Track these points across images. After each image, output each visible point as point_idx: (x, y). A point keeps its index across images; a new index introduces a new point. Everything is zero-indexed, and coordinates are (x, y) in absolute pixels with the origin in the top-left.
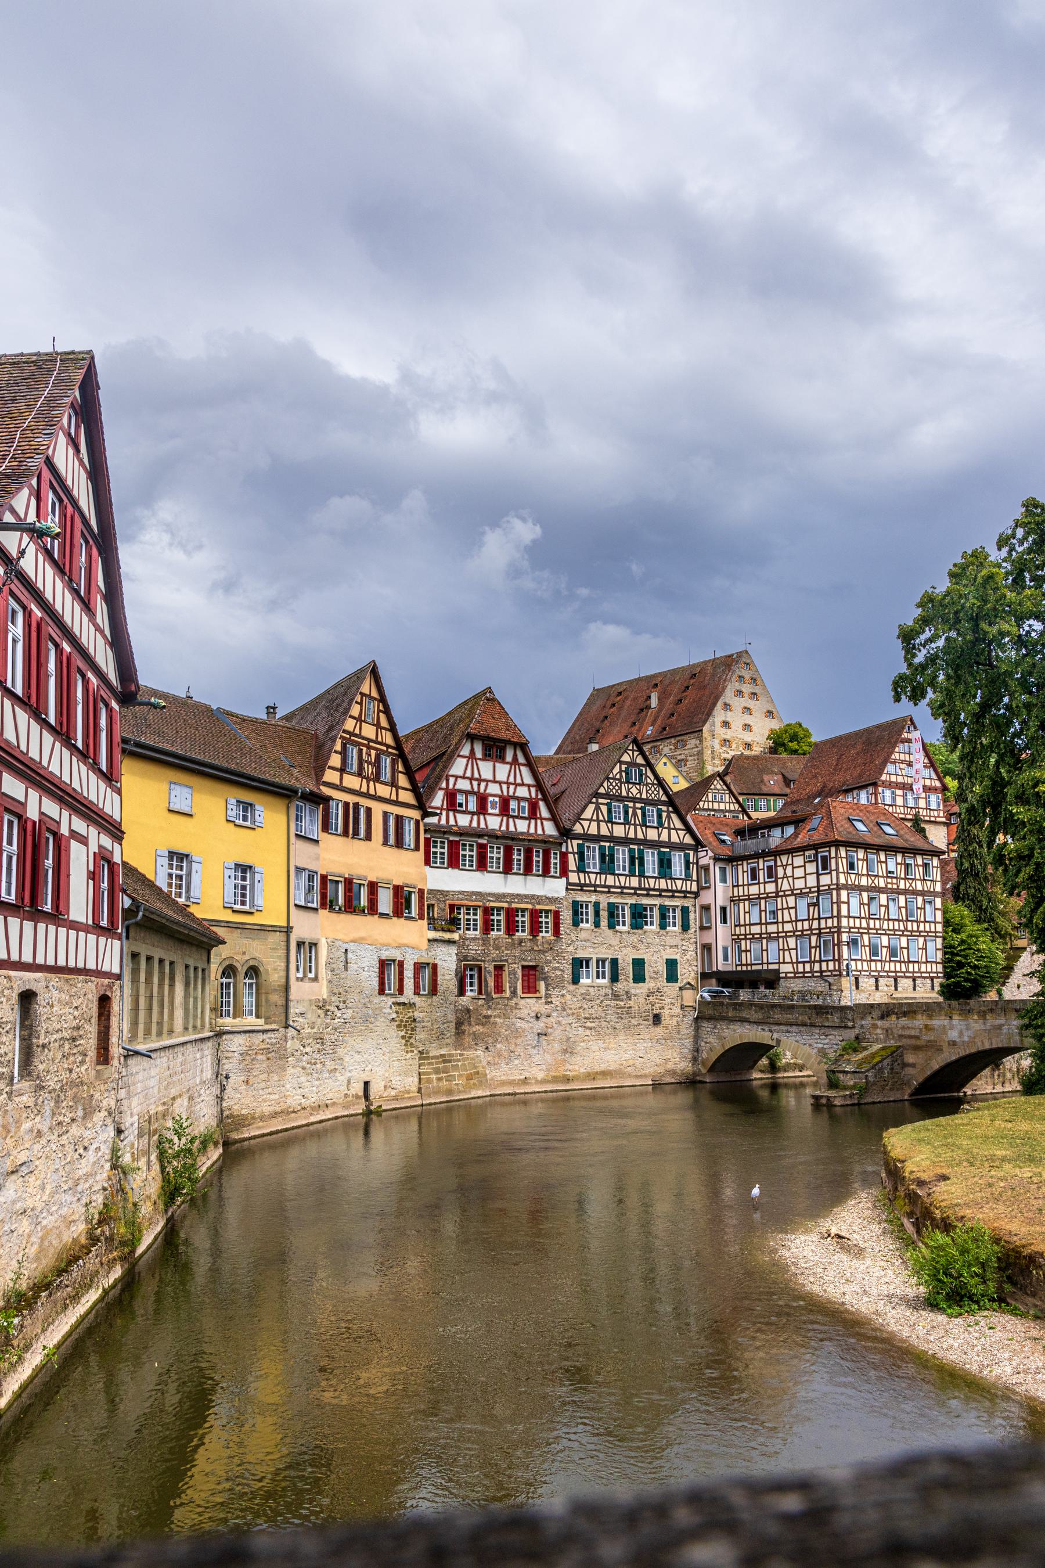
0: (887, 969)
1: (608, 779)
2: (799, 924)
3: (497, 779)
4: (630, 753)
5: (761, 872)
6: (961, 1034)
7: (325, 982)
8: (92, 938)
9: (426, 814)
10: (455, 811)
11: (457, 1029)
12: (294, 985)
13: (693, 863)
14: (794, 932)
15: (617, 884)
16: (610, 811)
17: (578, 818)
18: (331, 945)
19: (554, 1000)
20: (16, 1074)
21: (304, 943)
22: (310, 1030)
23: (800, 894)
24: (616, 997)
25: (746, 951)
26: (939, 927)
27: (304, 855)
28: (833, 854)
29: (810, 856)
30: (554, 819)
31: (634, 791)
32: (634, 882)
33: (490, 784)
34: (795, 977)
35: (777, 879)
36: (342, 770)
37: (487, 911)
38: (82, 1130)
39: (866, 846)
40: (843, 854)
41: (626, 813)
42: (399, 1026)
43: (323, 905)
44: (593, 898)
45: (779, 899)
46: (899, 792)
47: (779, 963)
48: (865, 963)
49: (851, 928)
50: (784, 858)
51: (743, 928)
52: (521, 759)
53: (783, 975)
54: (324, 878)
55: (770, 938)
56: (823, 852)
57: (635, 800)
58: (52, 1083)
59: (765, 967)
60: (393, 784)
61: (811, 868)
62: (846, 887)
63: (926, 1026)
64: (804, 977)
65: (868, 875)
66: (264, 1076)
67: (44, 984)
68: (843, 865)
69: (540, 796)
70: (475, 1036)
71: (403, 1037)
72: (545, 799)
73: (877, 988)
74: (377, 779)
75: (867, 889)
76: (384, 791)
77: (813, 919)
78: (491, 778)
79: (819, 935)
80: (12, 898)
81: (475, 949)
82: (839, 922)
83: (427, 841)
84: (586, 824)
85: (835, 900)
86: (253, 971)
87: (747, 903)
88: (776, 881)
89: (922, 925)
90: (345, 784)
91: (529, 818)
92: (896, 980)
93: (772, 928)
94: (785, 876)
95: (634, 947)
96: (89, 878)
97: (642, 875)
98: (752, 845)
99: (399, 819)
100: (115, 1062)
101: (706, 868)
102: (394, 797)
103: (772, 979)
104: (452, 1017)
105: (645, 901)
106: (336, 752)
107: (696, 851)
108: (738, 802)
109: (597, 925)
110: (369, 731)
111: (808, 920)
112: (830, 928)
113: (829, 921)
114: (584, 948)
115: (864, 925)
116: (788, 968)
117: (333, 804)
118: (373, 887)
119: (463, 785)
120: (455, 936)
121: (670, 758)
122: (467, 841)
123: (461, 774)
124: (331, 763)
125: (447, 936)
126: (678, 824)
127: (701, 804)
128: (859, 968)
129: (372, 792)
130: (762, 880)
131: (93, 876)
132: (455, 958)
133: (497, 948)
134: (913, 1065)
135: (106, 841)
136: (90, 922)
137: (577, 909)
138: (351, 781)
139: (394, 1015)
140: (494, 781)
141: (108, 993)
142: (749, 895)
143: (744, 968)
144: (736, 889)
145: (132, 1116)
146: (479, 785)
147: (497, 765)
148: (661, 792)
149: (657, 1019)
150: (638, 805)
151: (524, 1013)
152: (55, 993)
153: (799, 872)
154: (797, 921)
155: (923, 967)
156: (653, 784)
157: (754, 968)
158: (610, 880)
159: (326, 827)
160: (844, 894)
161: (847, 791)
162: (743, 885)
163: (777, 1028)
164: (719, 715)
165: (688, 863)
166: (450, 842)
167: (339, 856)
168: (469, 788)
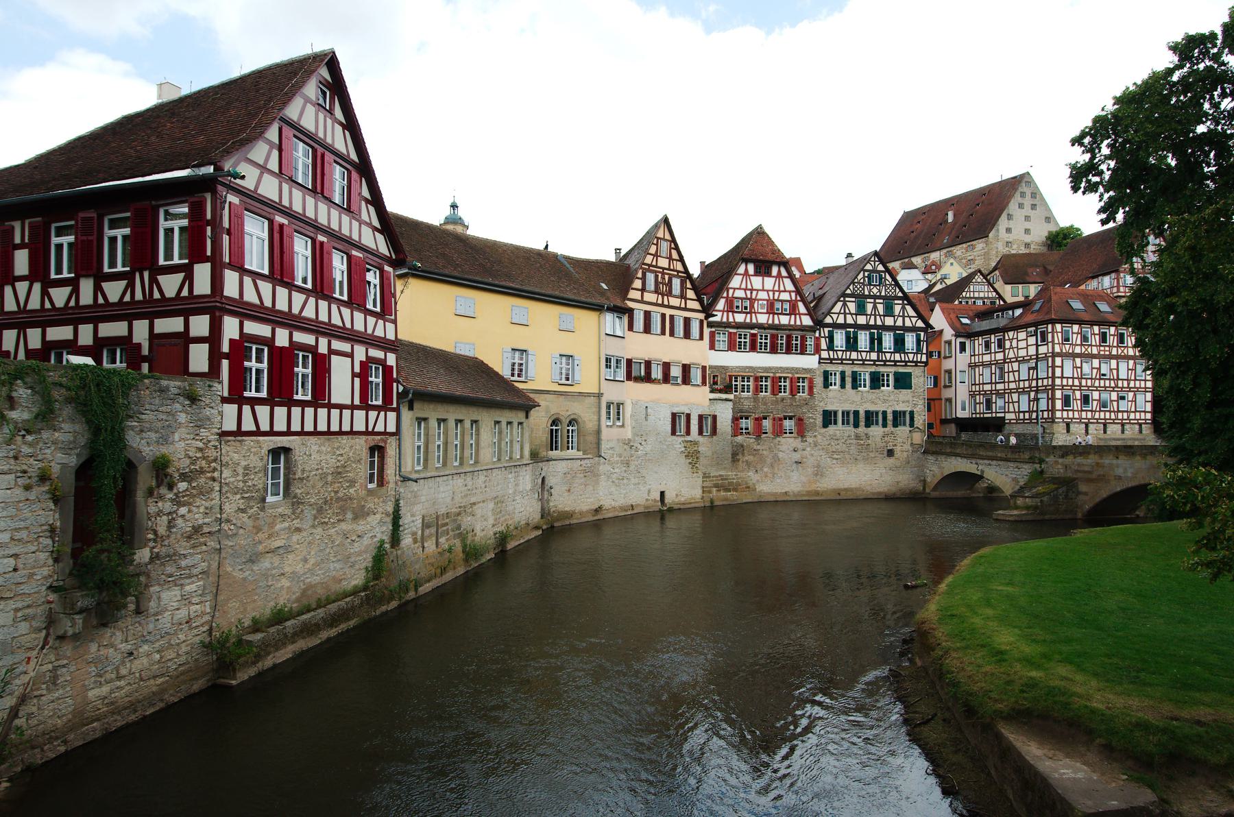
1: (853, 283)
6: (1125, 470)
9: (708, 316)
10: (733, 312)
12: (605, 433)
17: (829, 313)
18: (634, 404)
23: (1024, 361)
24: (857, 437)
30: (809, 314)
31: (875, 291)
32: (874, 356)
37: (757, 379)
38: (355, 526)
39: (1080, 322)
43: (629, 377)
44: (840, 368)
50: (1011, 334)
52: (784, 273)
54: (629, 362)
56: (1042, 328)
60: (683, 296)
61: (1032, 340)
62: (1059, 355)
65: (1081, 345)
68: (1058, 338)
70: (748, 463)
72: (803, 300)
74: (670, 294)
75: (1080, 355)
76: (675, 302)
79: (1037, 392)
81: (747, 405)
82: (1053, 381)
83: (712, 335)
84: (835, 316)
91: (790, 314)
92: (1105, 425)
93: (1000, 387)
97: (880, 351)
98: (985, 325)
100: (392, 485)
101: (949, 343)
103: (998, 425)
105: (882, 369)
114: (832, 403)
116: (1012, 416)
118: (666, 366)
122: (743, 331)
133: (765, 404)
134: (1086, 494)
137: (826, 375)
138: (650, 297)
145: (412, 516)
149: (890, 453)
151: (784, 448)
153: (1022, 344)
158: (854, 355)
159: (631, 328)
160: (1058, 361)
161: (1093, 278)
165: (918, 341)
166: (730, 334)
167: (641, 346)
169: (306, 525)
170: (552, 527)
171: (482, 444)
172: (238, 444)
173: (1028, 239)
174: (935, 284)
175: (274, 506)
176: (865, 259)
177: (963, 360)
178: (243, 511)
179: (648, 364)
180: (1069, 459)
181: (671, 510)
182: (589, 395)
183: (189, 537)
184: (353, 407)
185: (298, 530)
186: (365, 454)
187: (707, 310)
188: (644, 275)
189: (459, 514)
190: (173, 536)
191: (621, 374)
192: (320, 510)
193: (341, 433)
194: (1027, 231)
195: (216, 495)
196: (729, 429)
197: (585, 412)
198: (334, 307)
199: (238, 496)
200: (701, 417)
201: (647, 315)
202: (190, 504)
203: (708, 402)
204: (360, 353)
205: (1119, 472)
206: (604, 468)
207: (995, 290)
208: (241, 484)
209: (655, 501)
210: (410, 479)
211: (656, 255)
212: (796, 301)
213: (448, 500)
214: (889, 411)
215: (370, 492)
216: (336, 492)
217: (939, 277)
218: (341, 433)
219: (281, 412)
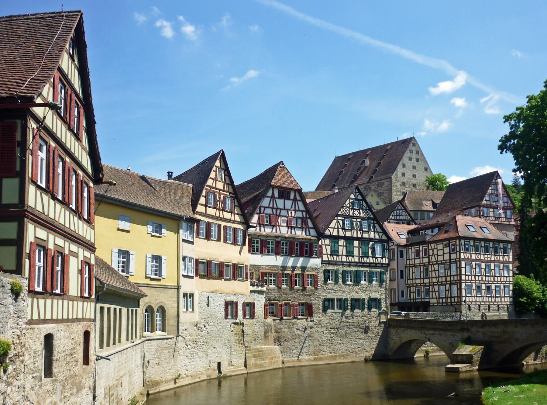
0: (484, 300)
1: (343, 207)
2: (440, 279)
3: (286, 208)
4: (355, 193)
5: (421, 253)
7: (198, 313)
8: (80, 303)
11: (265, 335)
13: (386, 249)
14: (437, 282)
15: (348, 260)
16: (344, 223)
19: (315, 319)
20: (43, 375)
21: (187, 294)
22: (190, 337)
23: (442, 264)
25: (413, 292)
26: (511, 279)
27: (186, 250)
28: (458, 243)
29: (446, 245)
30: (315, 227)
33: (282, 211)
34: (438, 305)
35: (429, 256)
36: (206, 206)
40: (463, 243)
41: (352, 224)
42: (235, 334)
44: (335, 268)
45: (430, 266)
46: (491, 210)
47: (430, 298)
48: (473, 298)
49: (466, 280)
50: (433, 245)
51: (411, 281)
52: (298, 198)
53: (432, 304)
54: (197, 261)
55: (425, 285)
56: (452, 242)
57: (357, 218)
58: (61, 377)
59: (423, 300)
61: (447, 250)
62: (464, 260)
63: (504, 331)
64: (442, 305)
65: (475, 254)
67: (56, 329)
69: (308, 216)
71: (237, 340)
73: (479, 310)
74: (224, 210)
76: (227, 216)
77: (447, 276)
78: (283, 207)
79: (450, 284)
80: (40, 289)
81: (275, 295)
82: (461, 277)
84: (331, 230)
85: (458, 266)
86: (162, 310)
87: (414, 268)
88: (429, 257)
89: (502, 278)
90: (208, 213)
93: (426, 281)
94: (433, 255)
95: (356, 292)
96: (78, 273)
98: (416, 239)
99: (235, 230)
102: (233, 219)
103: (425, 306)
104: (262, 329)
106: (203, 196)
107: (388, 244)
108: (410, 215)
109: (336, 282)
111: (445, 276)
112: (456, 281)
113: (456, 277)
115: (473, 279)
117: (202, 223)
120: (264, 289)
121: (375, 191)
123: (267, 206)
124: (200, 202)
125: (260, 289)
126: (379, 229)
127: (391, 217)
128: (471, 300)
130: (421, 257)
131: (81, 272)
132: (264, 299)
133: (286, 294)
135: (87, 254)
136: (79, 295)
137: (327, 275)
138: (211, 211)
139: (233, 329)
140: (284, 209)
141: (89, 330)
142: (415, 264)
143: (412, 301)
144: (408, 261)
146: (276, 211)
147: (286, 201)
148: (370, 213)
150: (358, 220)
152: (62, 333)
154: (439, 277)
155: (503, 298)
156: (366, 209)
157: (417, 301)
160: (463, 264)
162: (412, 259)
163: (428, 332)
164: (400, 169)
168: (271, 213)
173: (414, 181)
179: (209, 263)
181: (225, 377)
182: (171, 288)
187: (246, 223)
194: (414, 176)
197: (167, 300)
200: (245, 305)
203: (249, 293)
206: (181, 344)
209: (214, 370)
211: (215, 180)
212: (306, 218)
213: (113, 374)
214: (367, 298)
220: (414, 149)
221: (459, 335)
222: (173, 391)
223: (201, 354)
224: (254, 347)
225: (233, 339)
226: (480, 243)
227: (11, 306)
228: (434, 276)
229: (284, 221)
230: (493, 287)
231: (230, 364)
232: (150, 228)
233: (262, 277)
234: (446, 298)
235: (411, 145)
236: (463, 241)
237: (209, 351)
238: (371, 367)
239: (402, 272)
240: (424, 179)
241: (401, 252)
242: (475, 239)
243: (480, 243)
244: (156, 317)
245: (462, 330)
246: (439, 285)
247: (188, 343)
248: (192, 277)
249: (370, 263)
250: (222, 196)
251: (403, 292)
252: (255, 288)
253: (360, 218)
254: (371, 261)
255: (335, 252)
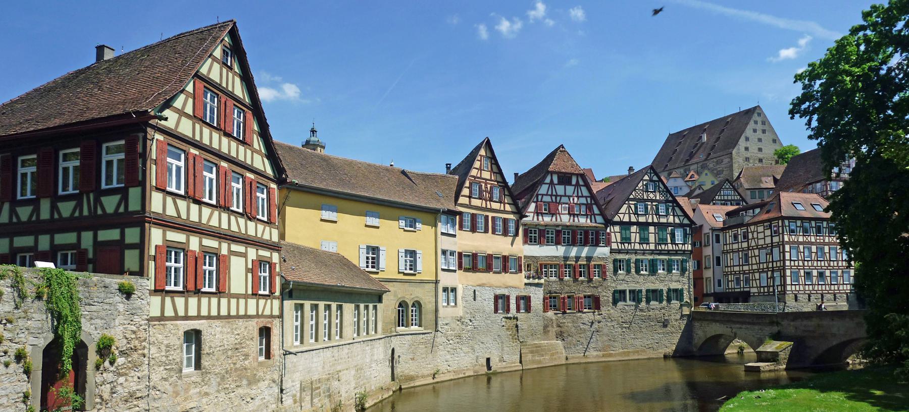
1: (635, 190)
12: (442, 312)
16: (636, 208)
19: (603, 312)
27: (445, 243)
30: (602, 214)
31: (651, 195)
36: (470, 197)
38: (248, 391)
40: (787, 224)
41: (646, 208)
42: (508, 329)
43: (460, 267)
44: (627, 257)
50: (752, 227)
52: (581, 183)
54: (460, 254)
56: (774, 223)
57: (652, 201)
61: (768, 232)
62: (788, 243)
66: (424, 356)
72: (597, 204)
73: (809, 300)
74: (491, 200)
76: (496, 206)
79: (773, 271)
81: (555, 287)
82: (784, 263)
84: (621, 216)
86: (418, 304)
92: (822, 295)
98: (734, 221)
99: (505, 221)
100: (277, 358)
104: (541, 323)
109: (628, 271)
110: (486, 175)
119: (547, 199)
120: (542, 281)
124: (463, 193)
125: (536, 281)
129: (489, 206)
138: (476, 202)
140: (565, 196)
145: (293, 381)
153: (761, 236)
159: (461, 228)
160: (787, 248)
169: (212, 390)
170: (400, 389)
171: (345, 324)
172: (161, 327)
174: (695, 189)
175: (188, 376)
176: (643, 172)
177: (719, 248)
178: (165, 379)
179: (475, 256)
180: (798, 323)
181: (495, 373)
182: (428, 282)
183: (126, 401)
184: (246, 296)
185: (207, 394)
186: (256, 333)
187: (520, 213)
188: (471, 184)
189: (328, 379)
190: (114, 400)
191: (453, 264)
192: (223, 378)
193: (238, 317)
194: (760, 150)
195: (145, 367)
196: (541, 307)
197: (424, 295)
198: (233, 218)
199: (162, 368)
200: (518, 298)
201: (473, 216)
202: (126, 374)
203: (523, 286)
204: (252, 253)
205: (834, 330)
207: (739, 194)
208: (164, 359)
209: (482, 366)
210: (290, 353)
211: (480, 169)
212: (591, 204)
213: (320, 369)
214: (665, 289)
215: (261, 364)
216: (235, 364)
217: (697, 184)
218: (238, 317)
219: (193, 301)
220: (759, 119)
221: (768, 330)
222: (431, 386)
223: (465, 349)
224: (530, 342)
225: (504, 333)
226: (810, 223)
227: (121, 305)
228: (754, 262)
229: (565, 208)
230: (828, 273)
231: (502, 360)
232: (402, 223)
233: (539, 268)
234: (768, 287)
235: (756, 115)
236: (786, 222)
237: (476, 346)
238: (671, 364)
239: (718, 259)
240: (774, 152)
241: (718, 237)
242: (802, 219)
243: (810, 223)
244: (406, 313)
245: (772, 323)
246: (760, 273)
247: (449, 338)
248: (455, 271)
249: (669, 251)
250: (489, 186)
251: (719, 281)
252: (531, 281)
253: (656, 201)
254: (670, 247)
255: (626, 240)
